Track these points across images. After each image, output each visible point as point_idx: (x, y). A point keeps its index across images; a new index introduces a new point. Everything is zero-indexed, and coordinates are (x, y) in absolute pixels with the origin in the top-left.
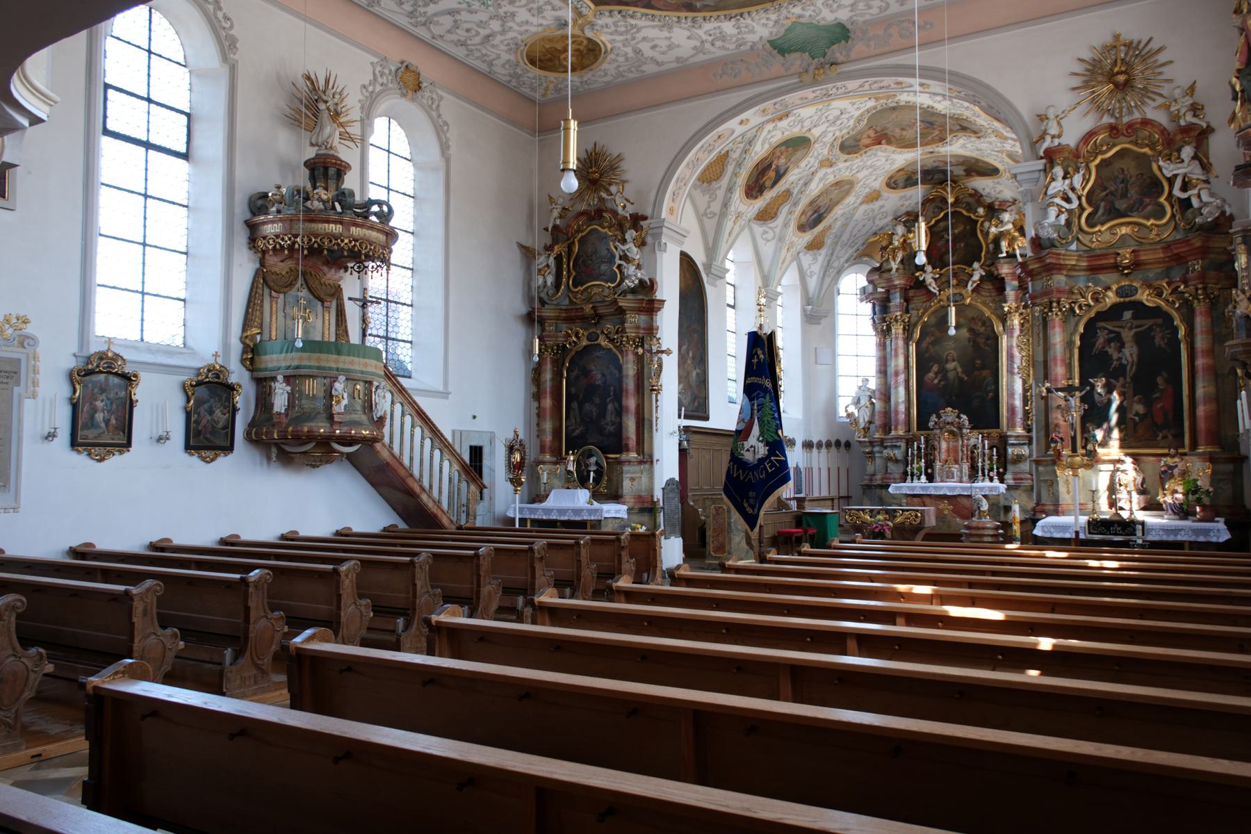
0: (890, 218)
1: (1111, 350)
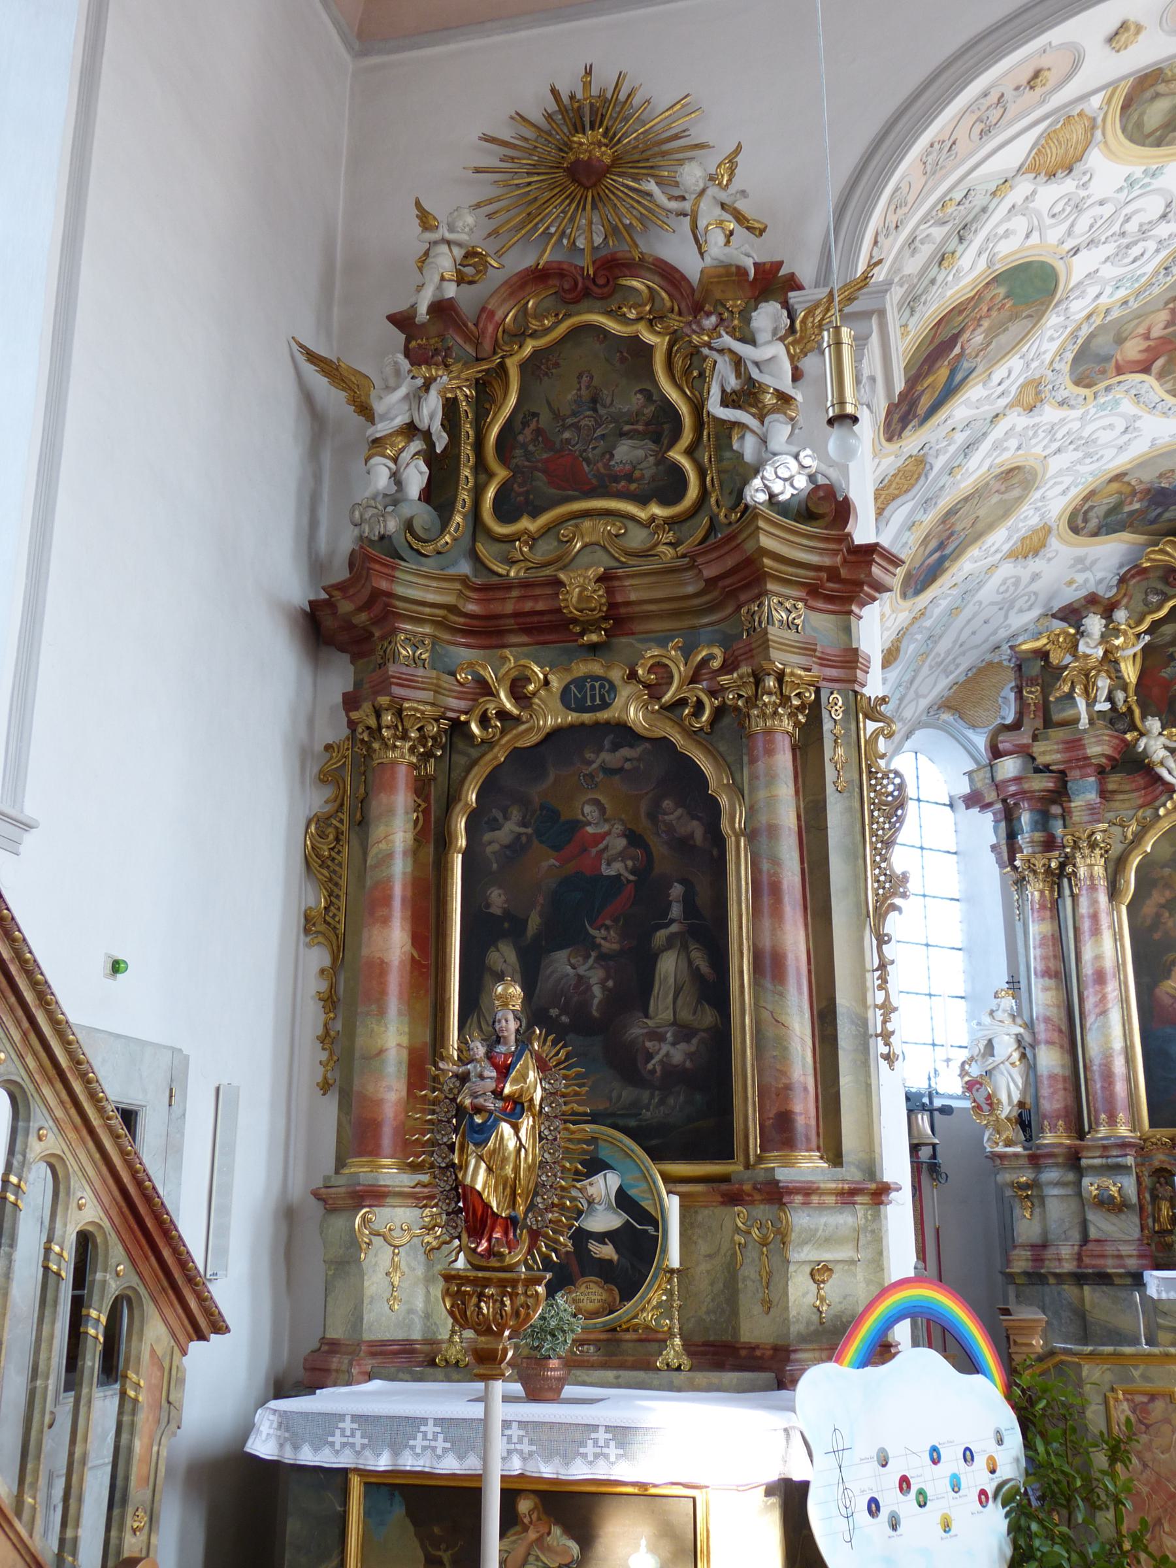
0: (1036, 612)
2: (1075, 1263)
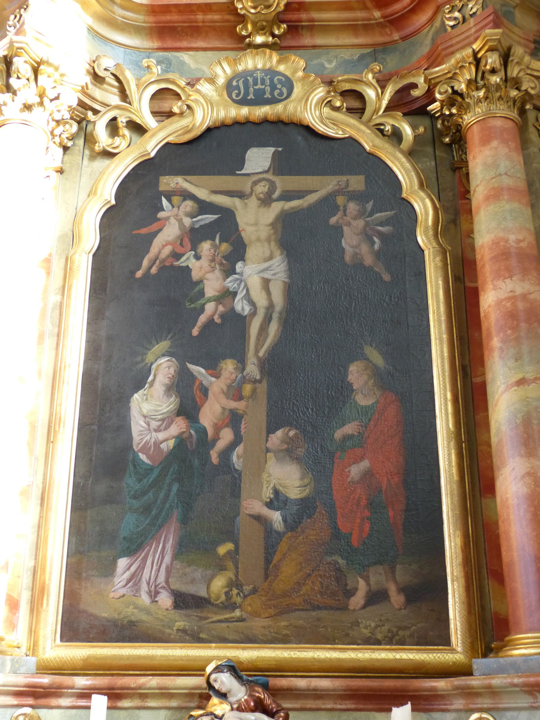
1: (201, 265)
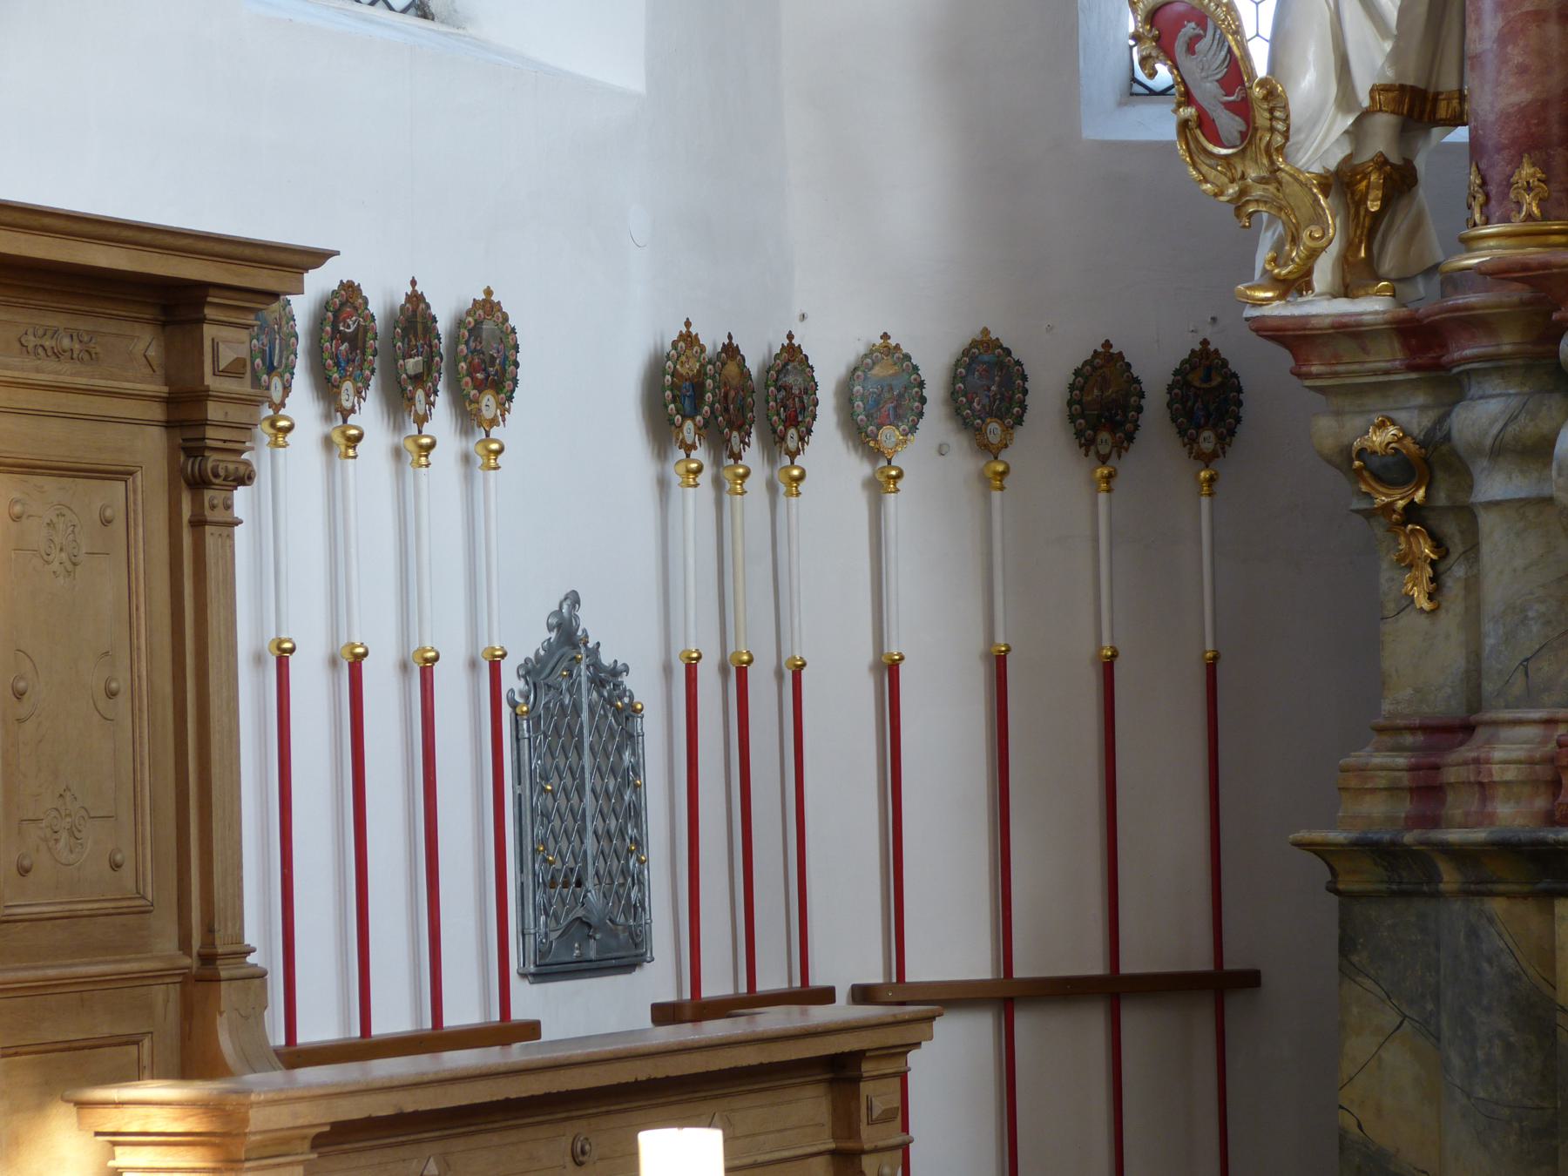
2: (1541, 803)
